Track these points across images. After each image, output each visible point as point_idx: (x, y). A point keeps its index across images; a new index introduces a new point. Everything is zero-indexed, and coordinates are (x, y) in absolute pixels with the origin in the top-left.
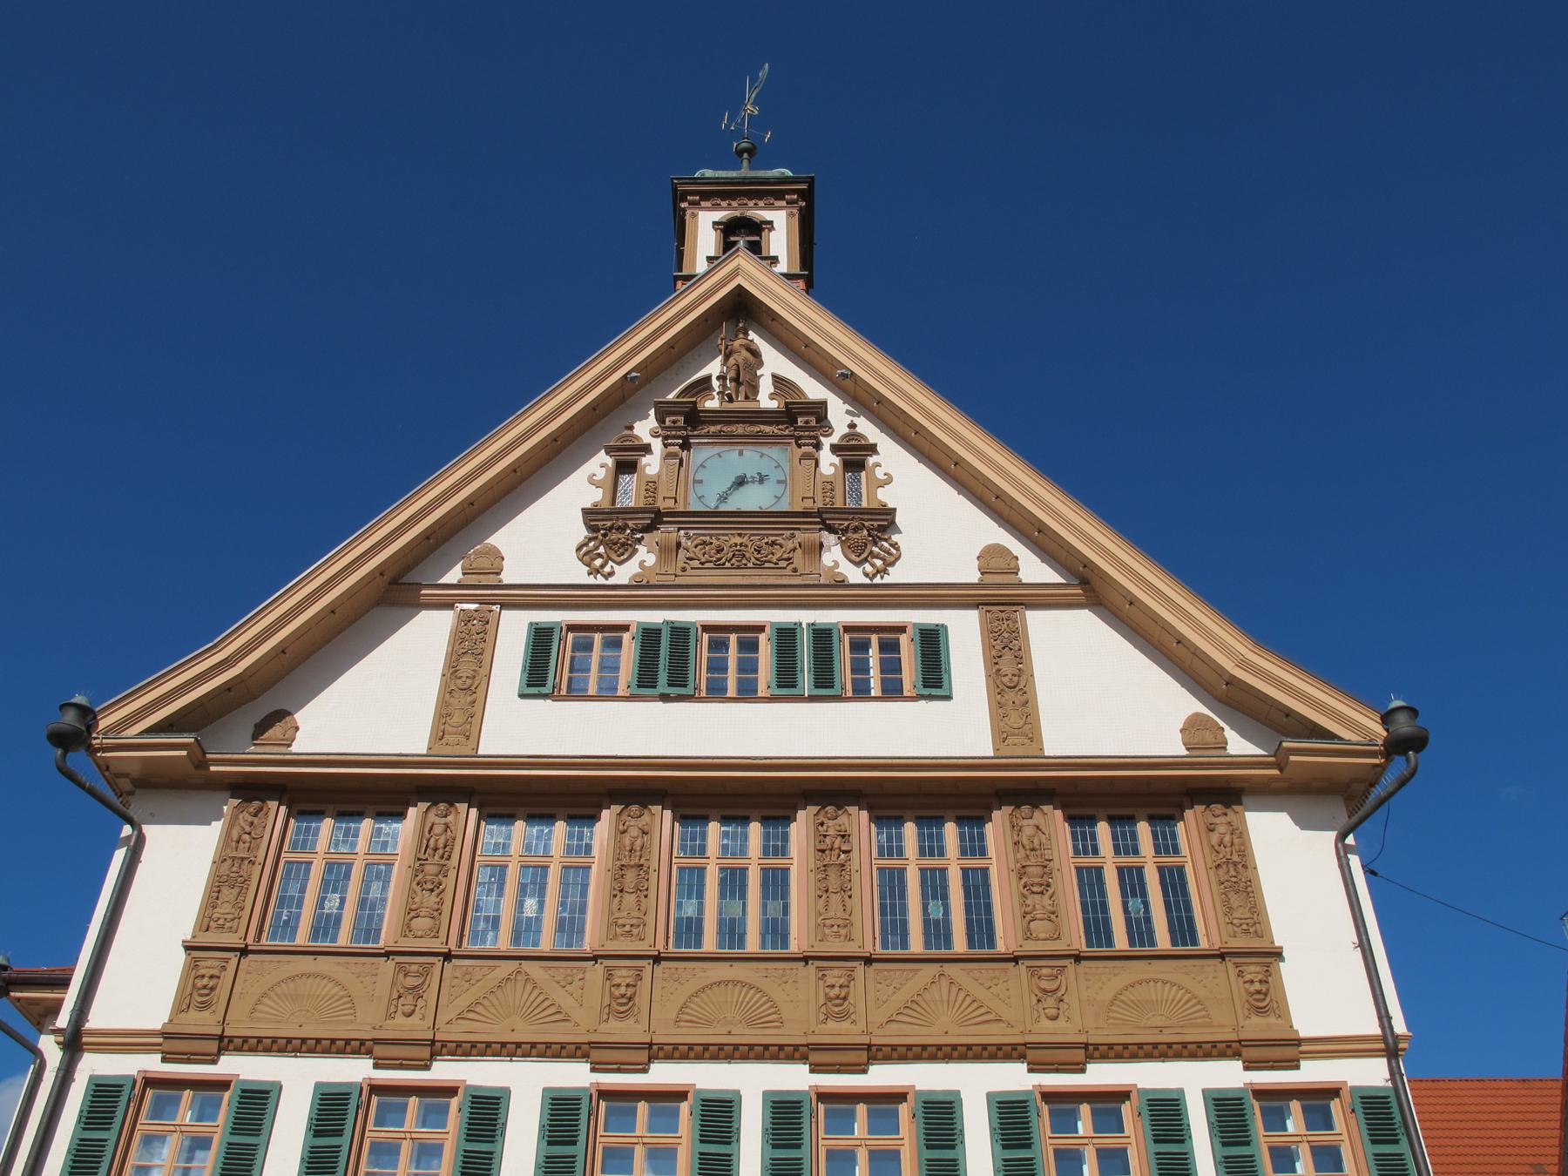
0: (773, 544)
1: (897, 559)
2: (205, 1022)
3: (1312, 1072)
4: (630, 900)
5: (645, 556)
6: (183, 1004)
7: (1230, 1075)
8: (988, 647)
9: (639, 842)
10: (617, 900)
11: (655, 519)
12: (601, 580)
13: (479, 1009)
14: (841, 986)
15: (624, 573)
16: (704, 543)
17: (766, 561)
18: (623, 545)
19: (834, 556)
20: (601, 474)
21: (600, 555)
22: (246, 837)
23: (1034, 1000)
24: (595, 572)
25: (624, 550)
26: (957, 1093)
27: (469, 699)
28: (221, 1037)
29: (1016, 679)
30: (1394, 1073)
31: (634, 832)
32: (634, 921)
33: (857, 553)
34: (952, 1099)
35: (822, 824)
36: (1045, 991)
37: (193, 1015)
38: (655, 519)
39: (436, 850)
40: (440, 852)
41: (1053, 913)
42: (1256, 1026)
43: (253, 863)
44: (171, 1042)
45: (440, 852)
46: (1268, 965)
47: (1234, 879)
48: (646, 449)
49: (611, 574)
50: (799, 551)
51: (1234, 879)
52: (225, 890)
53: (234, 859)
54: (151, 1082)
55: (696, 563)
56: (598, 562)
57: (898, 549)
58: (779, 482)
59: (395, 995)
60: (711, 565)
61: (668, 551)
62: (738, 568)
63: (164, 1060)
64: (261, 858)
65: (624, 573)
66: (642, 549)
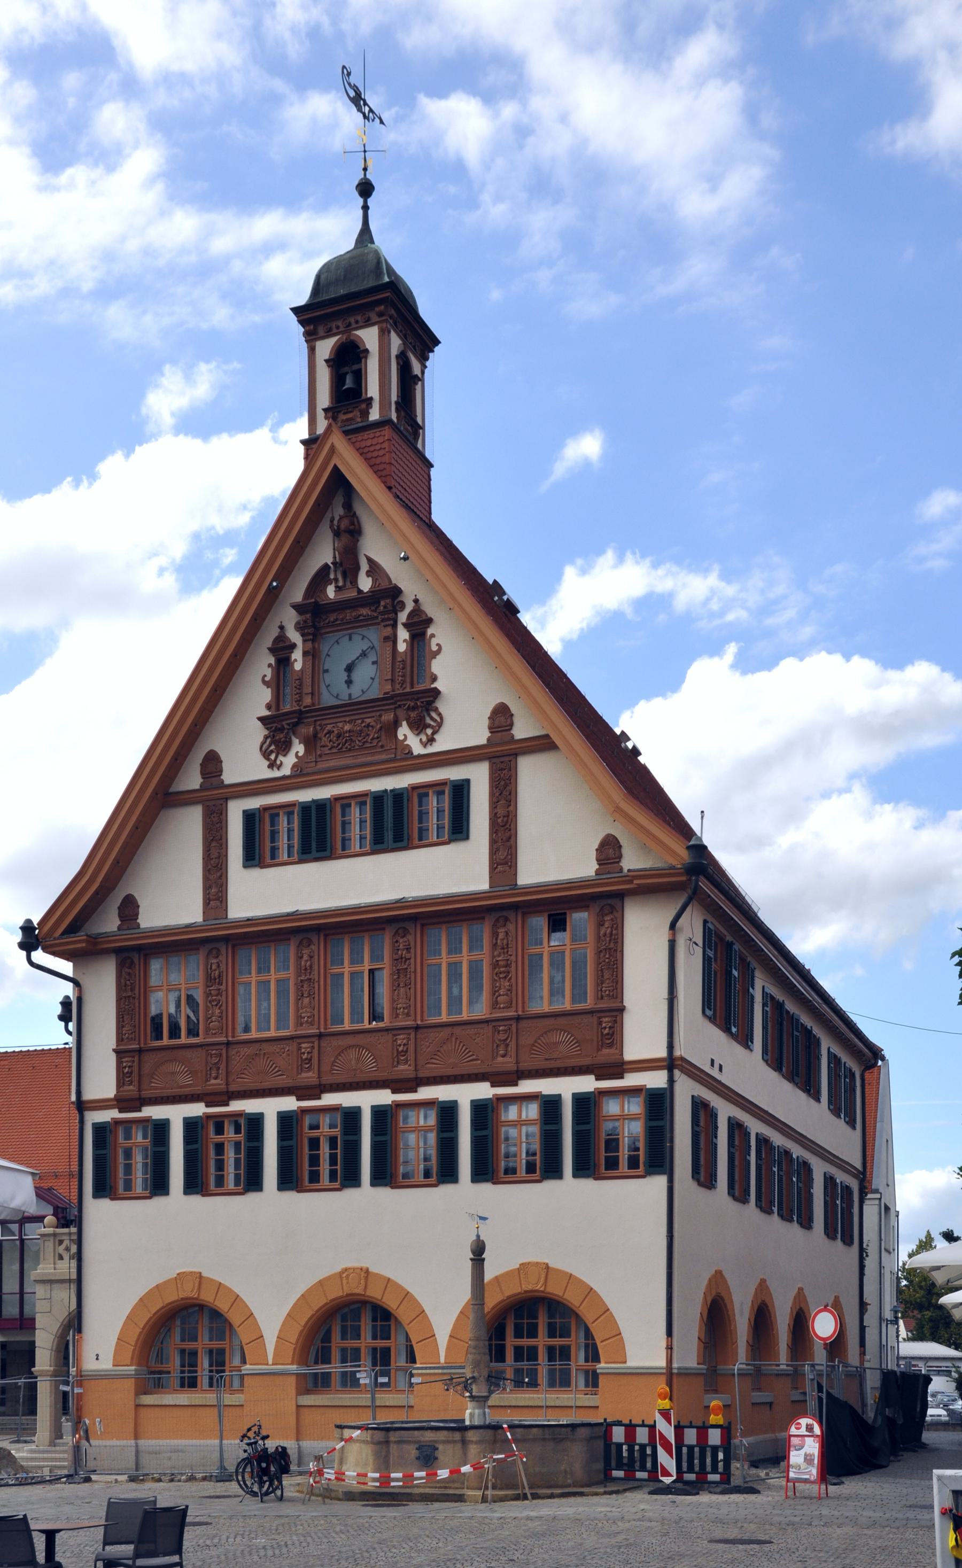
0: (368, 726)
1: (440, 725)
2: (131, 1090)
3: (631, 1080)
4: (306, 1001)
5: (298, 748)
6: (120, 1083)
7: (587, 1084)
8: (492, 794)
9: (308, 963)
10: (300, 1001)
11: (299, 717)
12: (276, 774)
13: (246, 1072)
14: (404, 1045)
15: (288, 762)
16: (330, 732)
17: (364, 742)
18: (284, 742)
19: (404, 731)
20: (269, 673)
21: (272, 752)
22: (128, 982)
23: (495, 1045)
24: (272, 766)
25: (284, 747)
26: (456, 1101)
27: (219, 874)
28: (140, 1099)
29: (505, 819)
30: (671, 1081)
31: (306, 957)
32: (309, 1014)
33: (418, 726)
34: (452, 1105)
35: (397, 942)
36: (500, 1040)
37: (126, 1088)
38: (299, 717)
39: (215, 979)
40: (217, 981)
41: (509, 990)
42: (606, 1055)
43: (134, 998)
44: (121, 1103)
45: (217, 981)
46: (616, 1016)
47: (607, 960)
48: (294, 646)
49: (279, 767)
50: (383, 729)
51: (607, 960)
52: (125, 1017)
53: (125, 997)
54: (117, 1122)
55: (326, 750)
56: (273, 757)
57: (441, 718)
58: (374, 663)
59: (208, 1068)
60: (334, 750)
61: (310, 743)
62: (350, 750)
63: (120, 1112)
64: (137, 997)
65: (288, 762)
66: (296, 741)
